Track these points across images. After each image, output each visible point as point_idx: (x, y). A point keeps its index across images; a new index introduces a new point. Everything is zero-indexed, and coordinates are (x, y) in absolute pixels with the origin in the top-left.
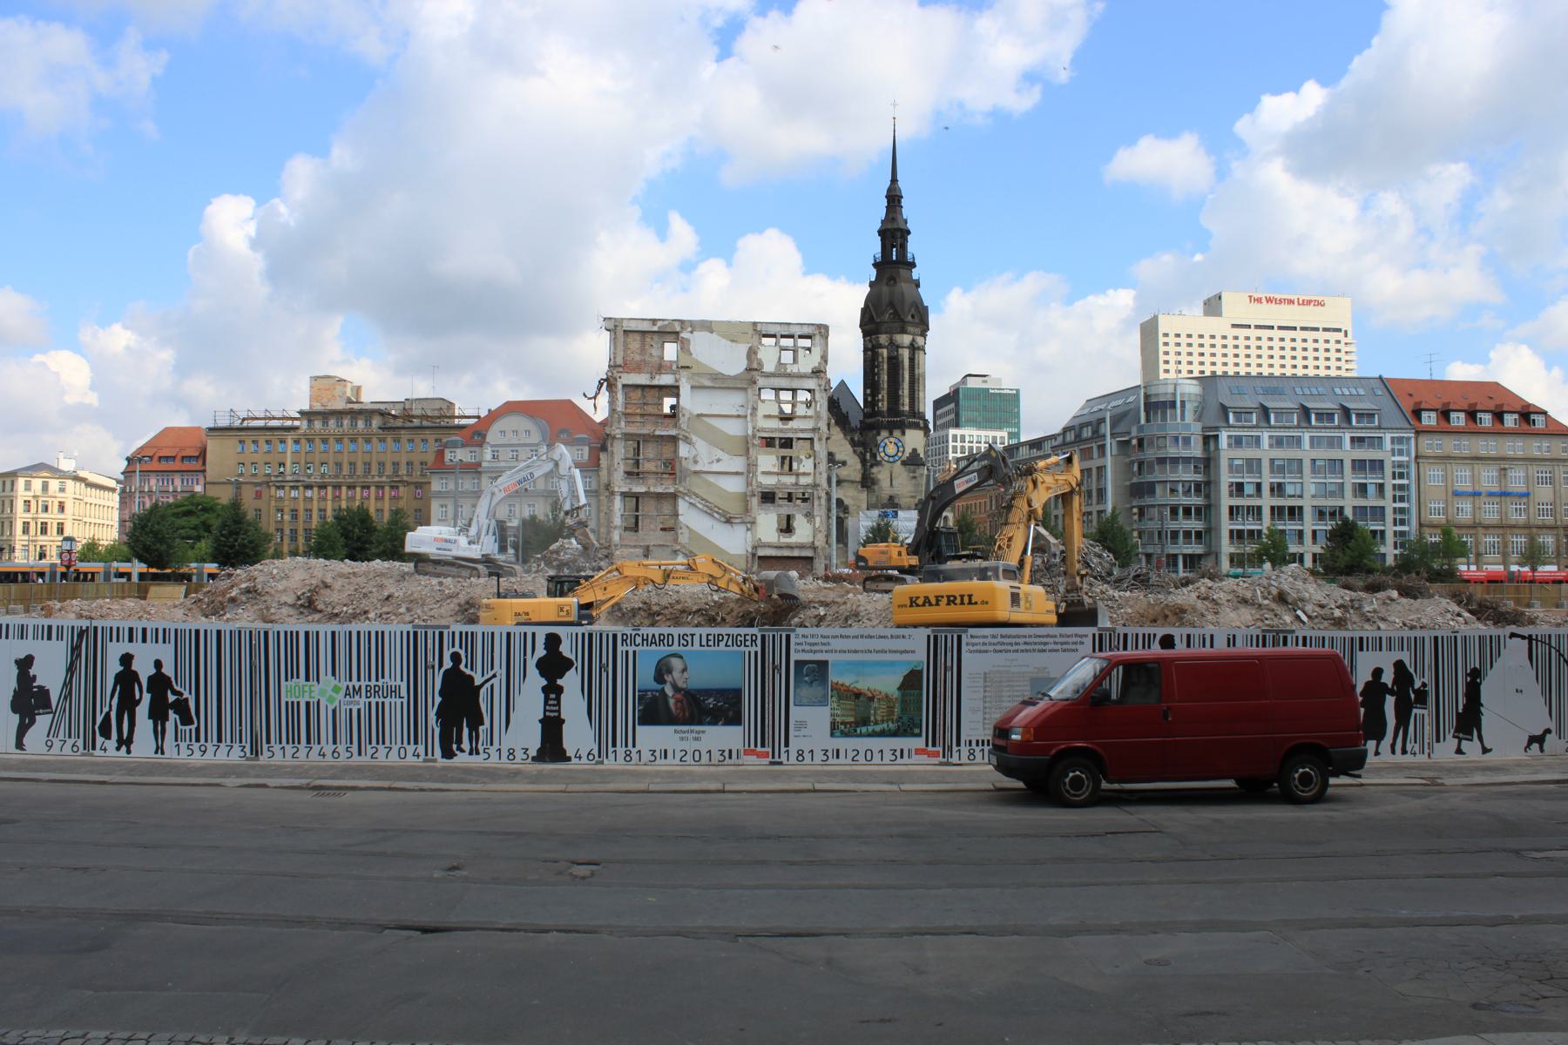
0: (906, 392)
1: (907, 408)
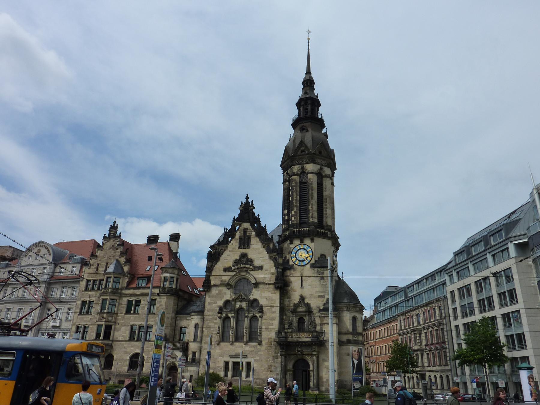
0: (315, 207)
1: (316, 220)
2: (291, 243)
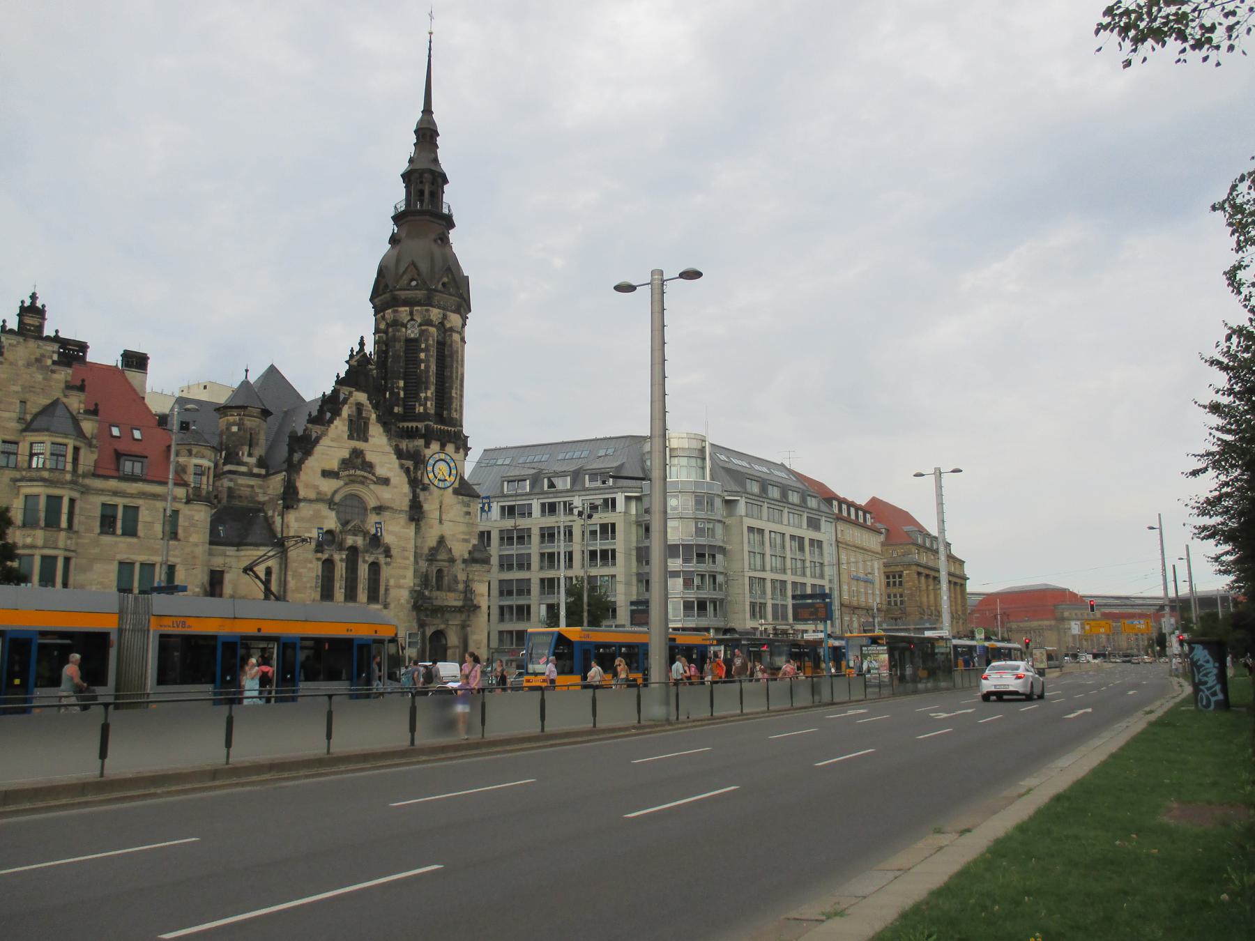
2: (427, 445)
